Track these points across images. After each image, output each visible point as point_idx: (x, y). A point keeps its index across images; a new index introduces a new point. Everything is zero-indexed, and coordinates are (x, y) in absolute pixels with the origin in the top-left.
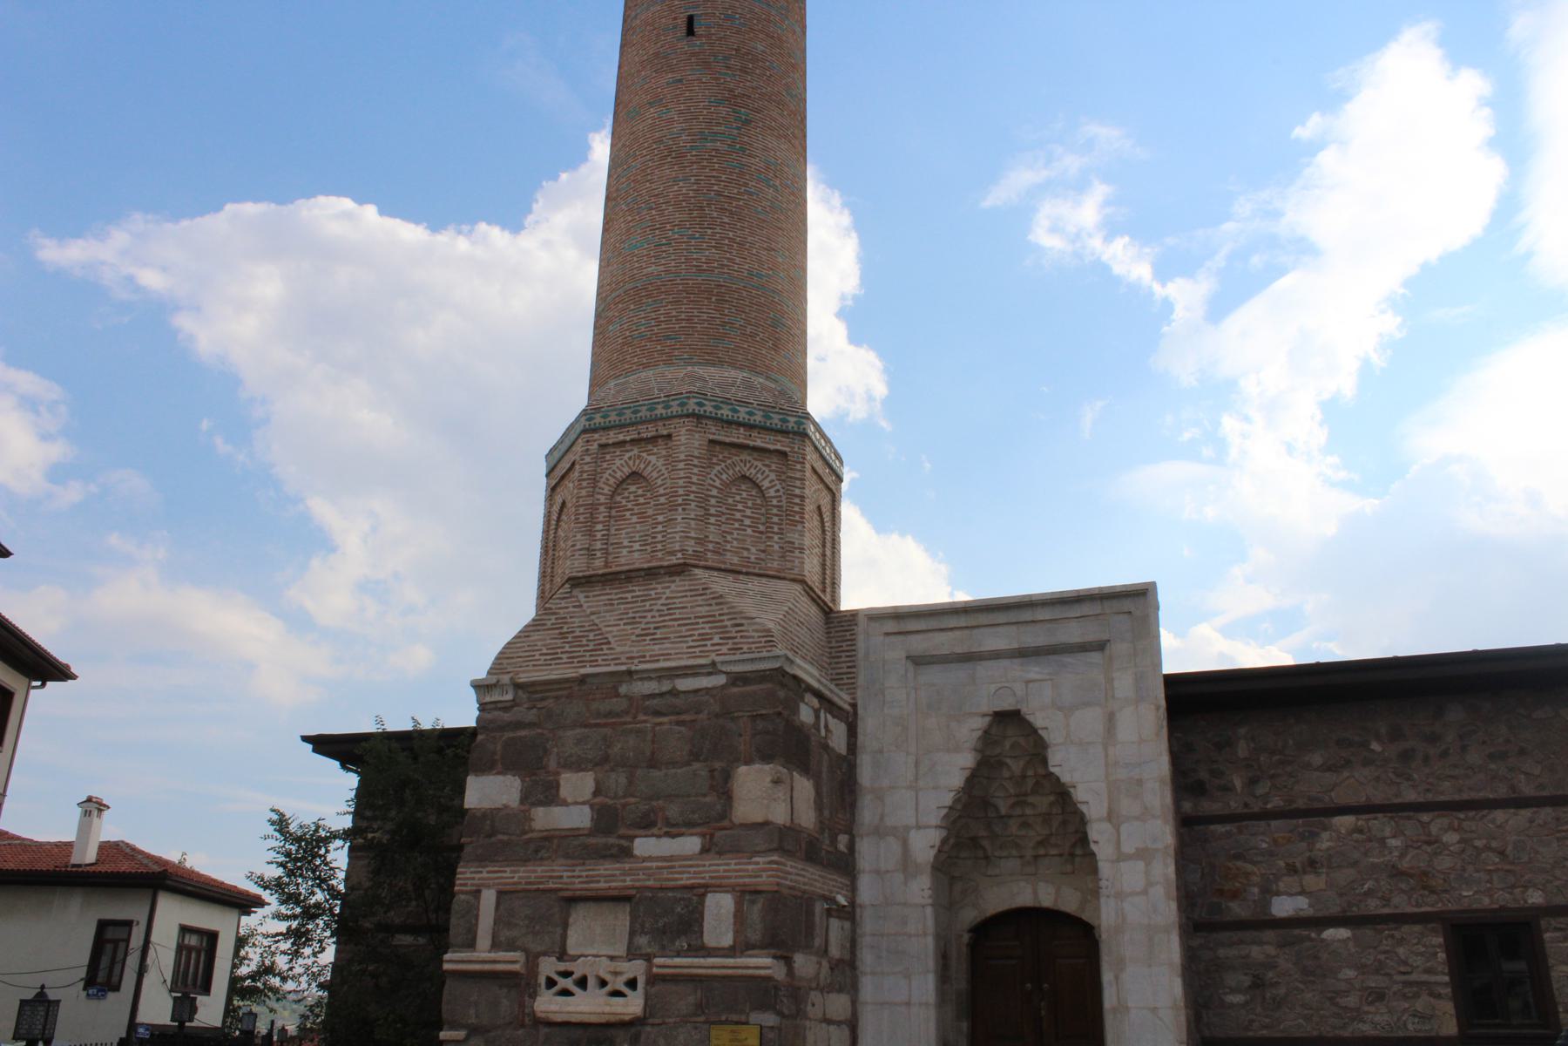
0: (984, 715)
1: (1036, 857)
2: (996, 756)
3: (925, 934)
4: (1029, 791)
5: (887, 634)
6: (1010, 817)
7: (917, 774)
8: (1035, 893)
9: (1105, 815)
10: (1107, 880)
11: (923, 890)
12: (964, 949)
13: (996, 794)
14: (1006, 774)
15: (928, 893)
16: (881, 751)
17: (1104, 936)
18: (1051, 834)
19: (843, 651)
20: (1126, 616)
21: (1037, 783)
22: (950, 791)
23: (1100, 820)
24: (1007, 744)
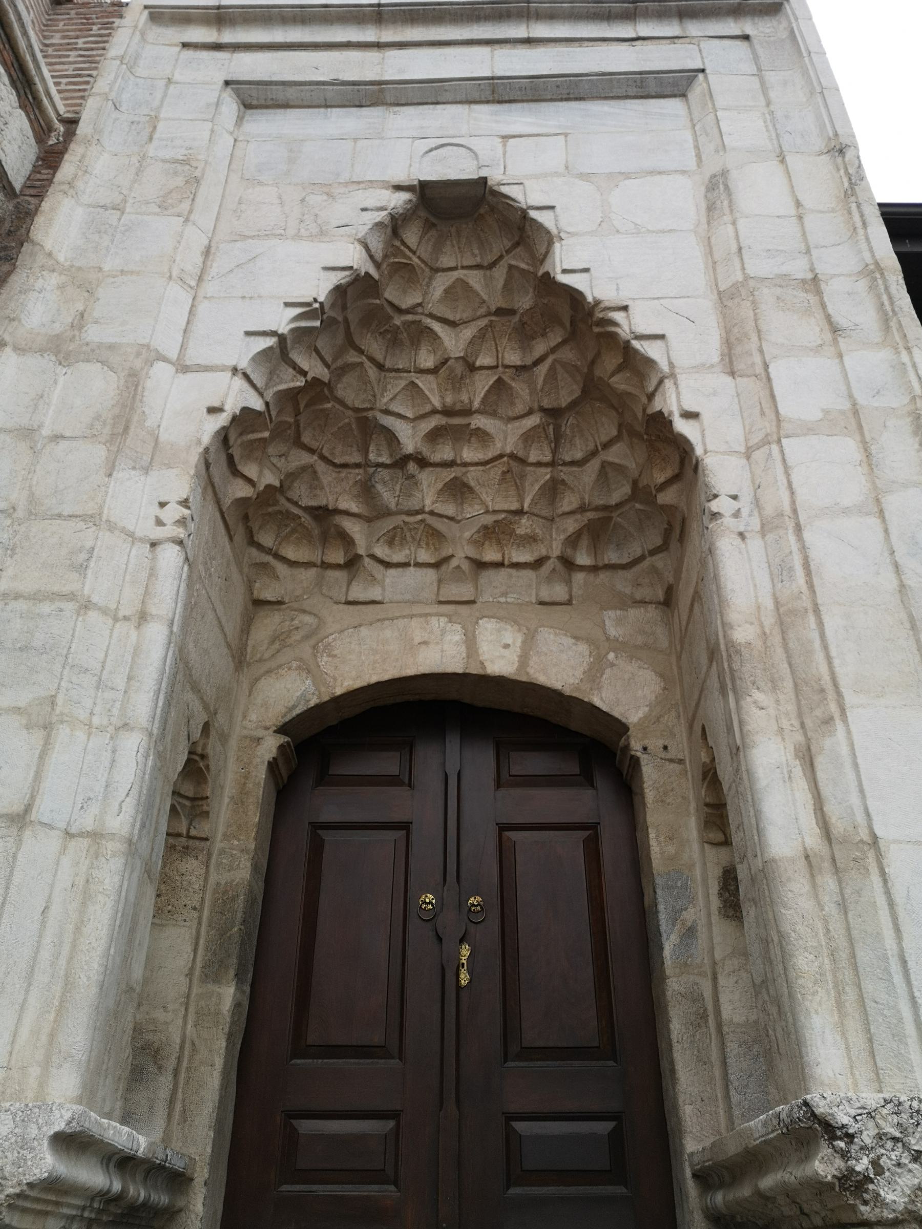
0: (398, 188)
1: (480, 565)
2: (408, 311)
3: (143, 617)
4: (476, 404)
5: (185, 45)
6: (423, 463)
7: (203, 271)
8: (471, 642)
9: (716, 359)
10: (735, 498)
11: (162, 505)
12: (261, 773)
13: (395, 407)
14: (427, 360)
15: (174, 512)
16: (119, 208)
17: (743, 633)
18: (520, 512)
19: (70, 63)
20: (738, 43)
21: (499, 381)
22: (287, 305)
23: (701, 368)
24: (440, 284)
